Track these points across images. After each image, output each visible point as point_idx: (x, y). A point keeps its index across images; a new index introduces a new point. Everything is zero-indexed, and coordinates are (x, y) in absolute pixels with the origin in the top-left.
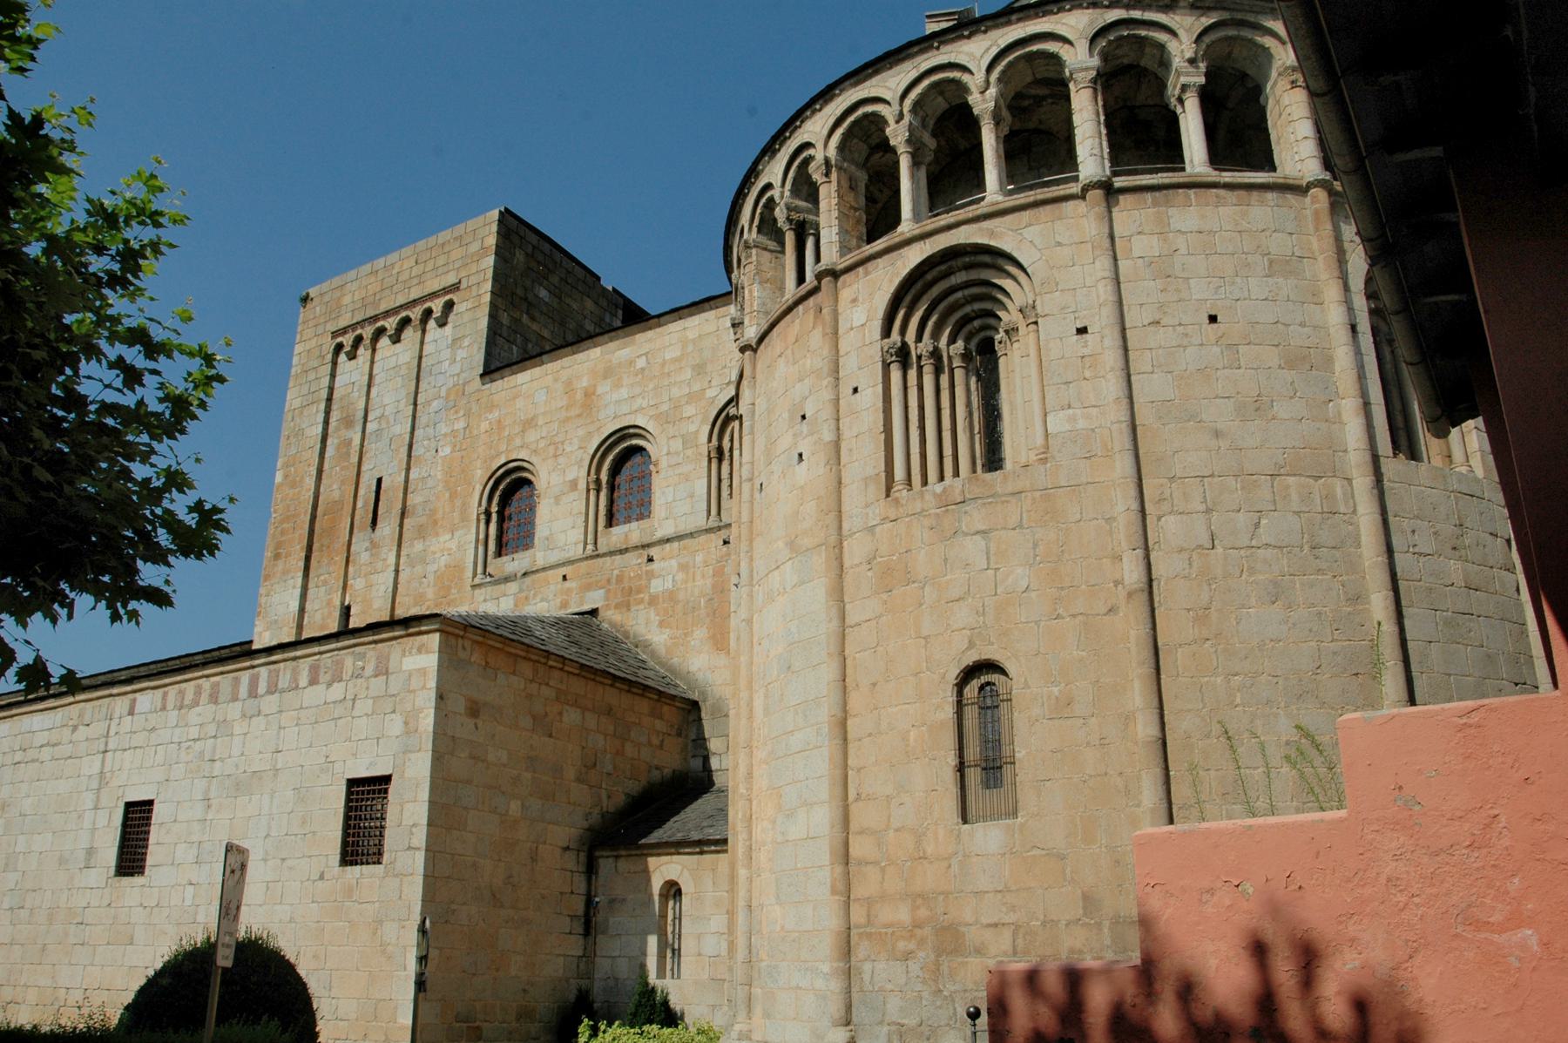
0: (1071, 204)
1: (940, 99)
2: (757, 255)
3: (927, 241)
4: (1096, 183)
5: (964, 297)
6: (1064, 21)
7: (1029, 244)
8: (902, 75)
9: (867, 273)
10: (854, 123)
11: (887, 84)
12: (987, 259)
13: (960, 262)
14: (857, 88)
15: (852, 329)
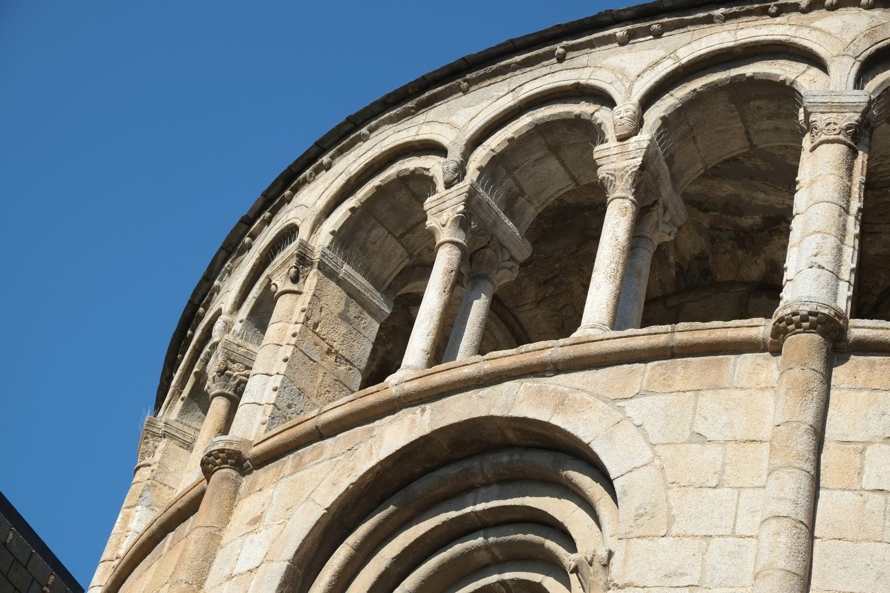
0: (748, 358)
1: (553, 164)
2: (165, 452)
3: (428, 406)
4: (804, 319)
5: (487, 547)
6: (817, 24)
7: (633, 430)
8: (485, 104)
9: (298, 467)
10: (380, 190)
11: (453, 119)
12: (542, 460)
13: (487, 465)
14: (401, 127)
15: (230, 577)
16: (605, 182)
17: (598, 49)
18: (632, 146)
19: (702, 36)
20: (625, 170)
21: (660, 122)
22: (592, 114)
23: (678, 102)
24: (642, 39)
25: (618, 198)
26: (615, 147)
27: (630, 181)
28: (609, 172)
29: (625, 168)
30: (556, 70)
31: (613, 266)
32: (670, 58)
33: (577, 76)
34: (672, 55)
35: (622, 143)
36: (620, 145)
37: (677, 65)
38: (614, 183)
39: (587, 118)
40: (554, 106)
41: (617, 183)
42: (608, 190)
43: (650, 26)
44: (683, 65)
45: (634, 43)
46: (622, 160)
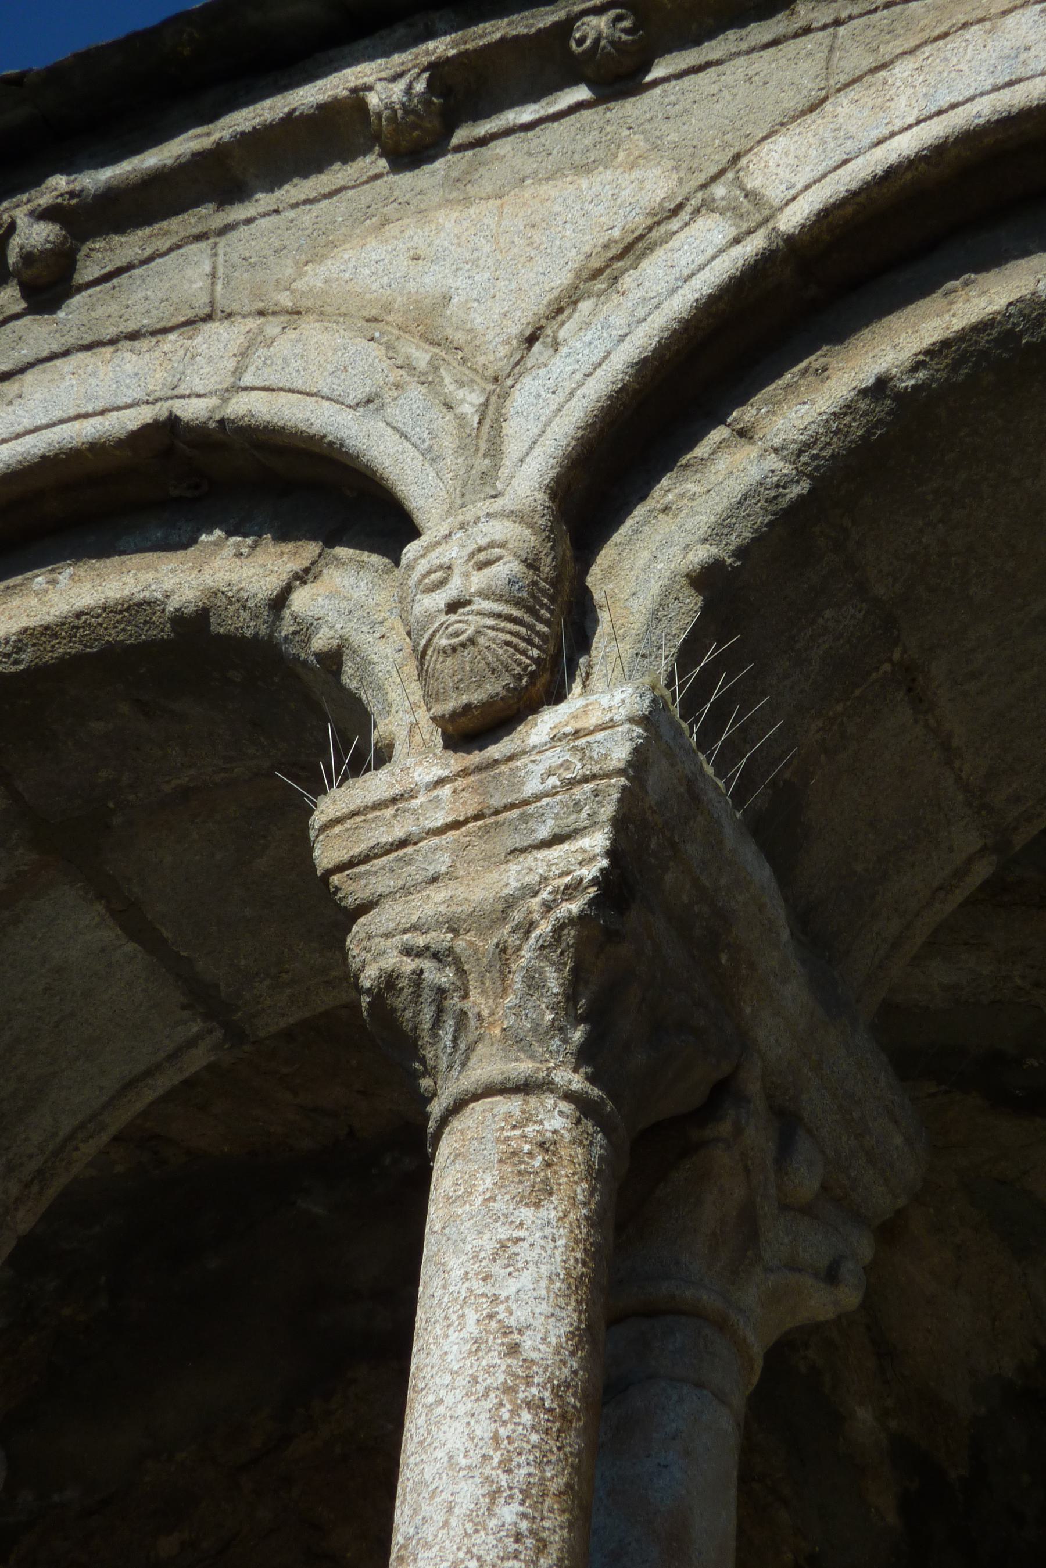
16: (399, 1002)
17: (264, 201)
18: (540, 769)
19: (887, 51)
20: (517, 915)
21: (693, 602)
22: (279, 602)
23: (787, 469)
24: (527, 114)
25: (490, 1091)
26: (440, 782)
27: (554, 982)
28: (421, 941)
29: (510, 903)
30: (26, 353)
31: (509, 1513)
32: (708, 206)
33: (157, 381)
34: (719, 190)
35: (476, 758)
36: (465, 773)
37: (755, 245)
38: (454, 1002)
39: (248, 626)
40: (40, 580)
41: (478, 1002)
42: (429, 1053)
43: (565, 28)
44: (789, 240)
45: (482, 142)
46: (492, 862)
